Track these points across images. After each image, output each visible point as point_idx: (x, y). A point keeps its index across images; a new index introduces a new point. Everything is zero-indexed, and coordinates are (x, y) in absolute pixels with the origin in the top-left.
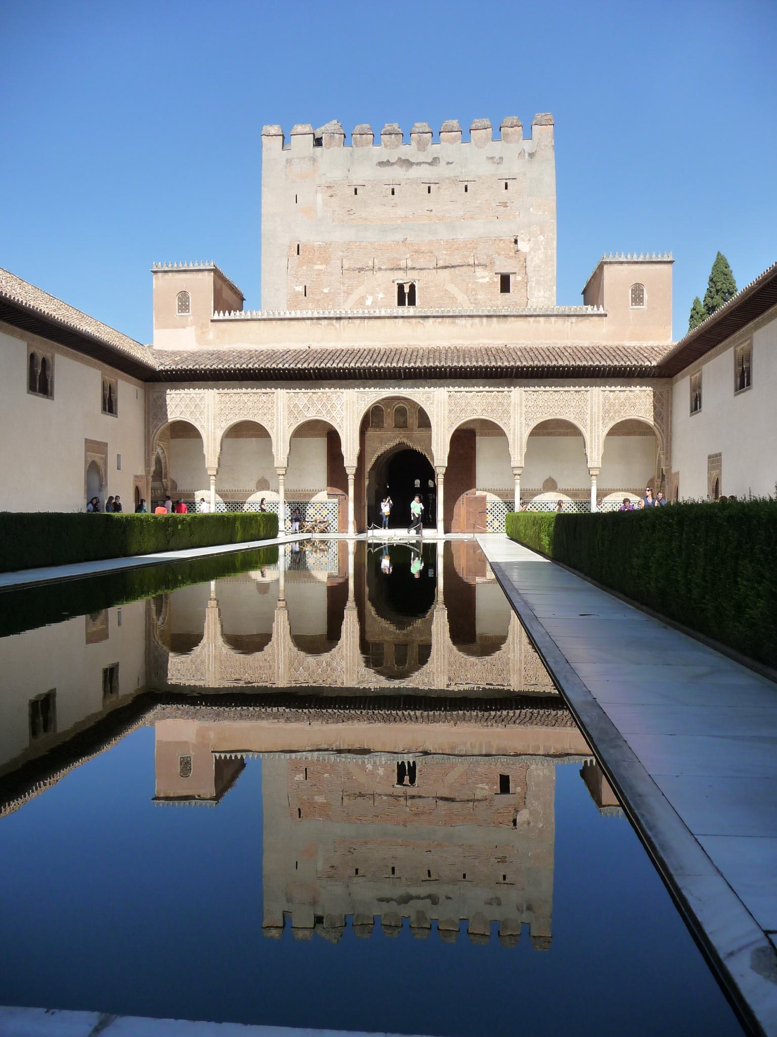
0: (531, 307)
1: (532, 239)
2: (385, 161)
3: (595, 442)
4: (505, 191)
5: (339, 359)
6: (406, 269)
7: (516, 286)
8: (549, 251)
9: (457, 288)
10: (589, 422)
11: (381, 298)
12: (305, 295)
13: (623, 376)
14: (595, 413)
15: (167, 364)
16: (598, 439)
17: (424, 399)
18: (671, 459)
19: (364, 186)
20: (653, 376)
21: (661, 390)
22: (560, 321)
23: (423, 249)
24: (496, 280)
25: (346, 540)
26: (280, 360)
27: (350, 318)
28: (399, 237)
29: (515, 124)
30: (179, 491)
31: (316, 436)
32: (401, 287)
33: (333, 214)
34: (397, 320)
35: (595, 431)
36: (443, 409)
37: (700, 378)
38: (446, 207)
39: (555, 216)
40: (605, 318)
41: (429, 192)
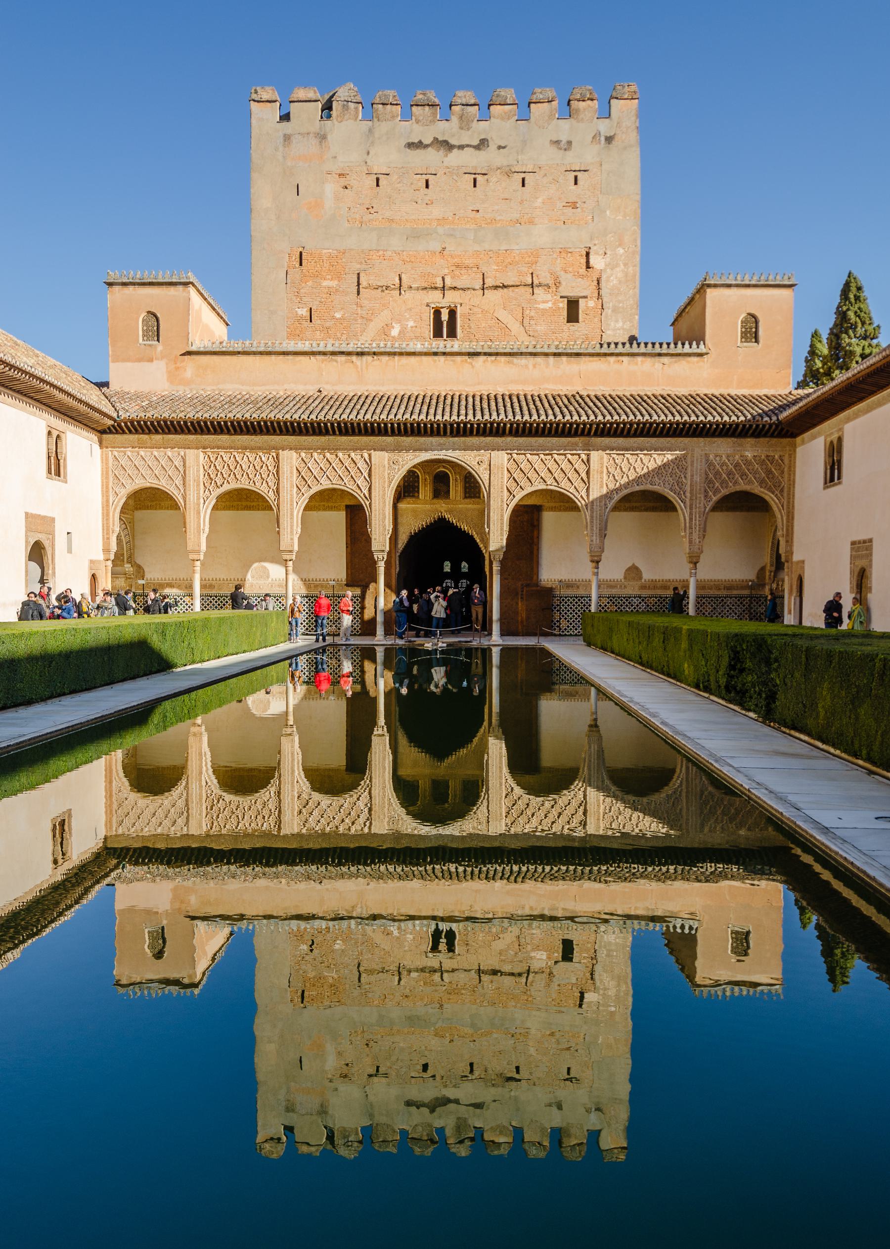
1: (608, 252)
2: (416, 141)
3: (695, 520)
5: (365, 408)
8: (631, 269)
10: (688, 495)
11: (412, 327)
12: (311, 321)
13: (733, 435)
14: (696, 483)
15: (131, 411)
16: (700, 517)
17: (476, 463)
18: (792, 542)
19: (388, 175)
20: (772, 436)
21: (781, 453)
22: (649, 361)
23: (469, 262)
24: (561, 305)
25: (376, 647)
26: (287, 409)
27: (374, 353)
29: (588, 96)
30: (147, 580)
31: (331, 509)
32: (437, 313)
34: (436, 358)
35: (696, 505)
36: (500, 476)
37: (840, 440)
38: (496, 207)
39: (639, 222)
41: (475, 186)
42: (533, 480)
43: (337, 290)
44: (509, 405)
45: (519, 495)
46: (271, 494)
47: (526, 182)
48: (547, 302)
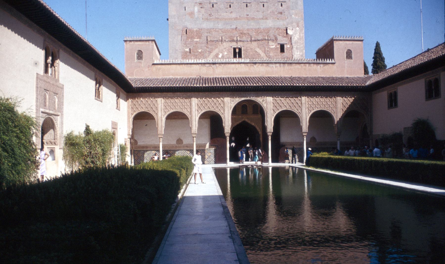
0: (295, 59)
1: (294, 29)
4: (281, 7)
6: (237, 41)
7: (287, 50)
8: (301, 35)
9: (260, 50)
11: (226, 54)
17: (261, 101)
19: (217, 3)
22: (315, 65)
26: (193, 83)
28: (234, 27)
32: (235, 49)
33: (203, 16)
36: (270, 105)
40: (335, 65)
42: (282, 107)
43: (199, 42)
44: (271, 80)
45: (277, 112)
46: (188, 113)
47: (265, 5)
48: (273, 45)
